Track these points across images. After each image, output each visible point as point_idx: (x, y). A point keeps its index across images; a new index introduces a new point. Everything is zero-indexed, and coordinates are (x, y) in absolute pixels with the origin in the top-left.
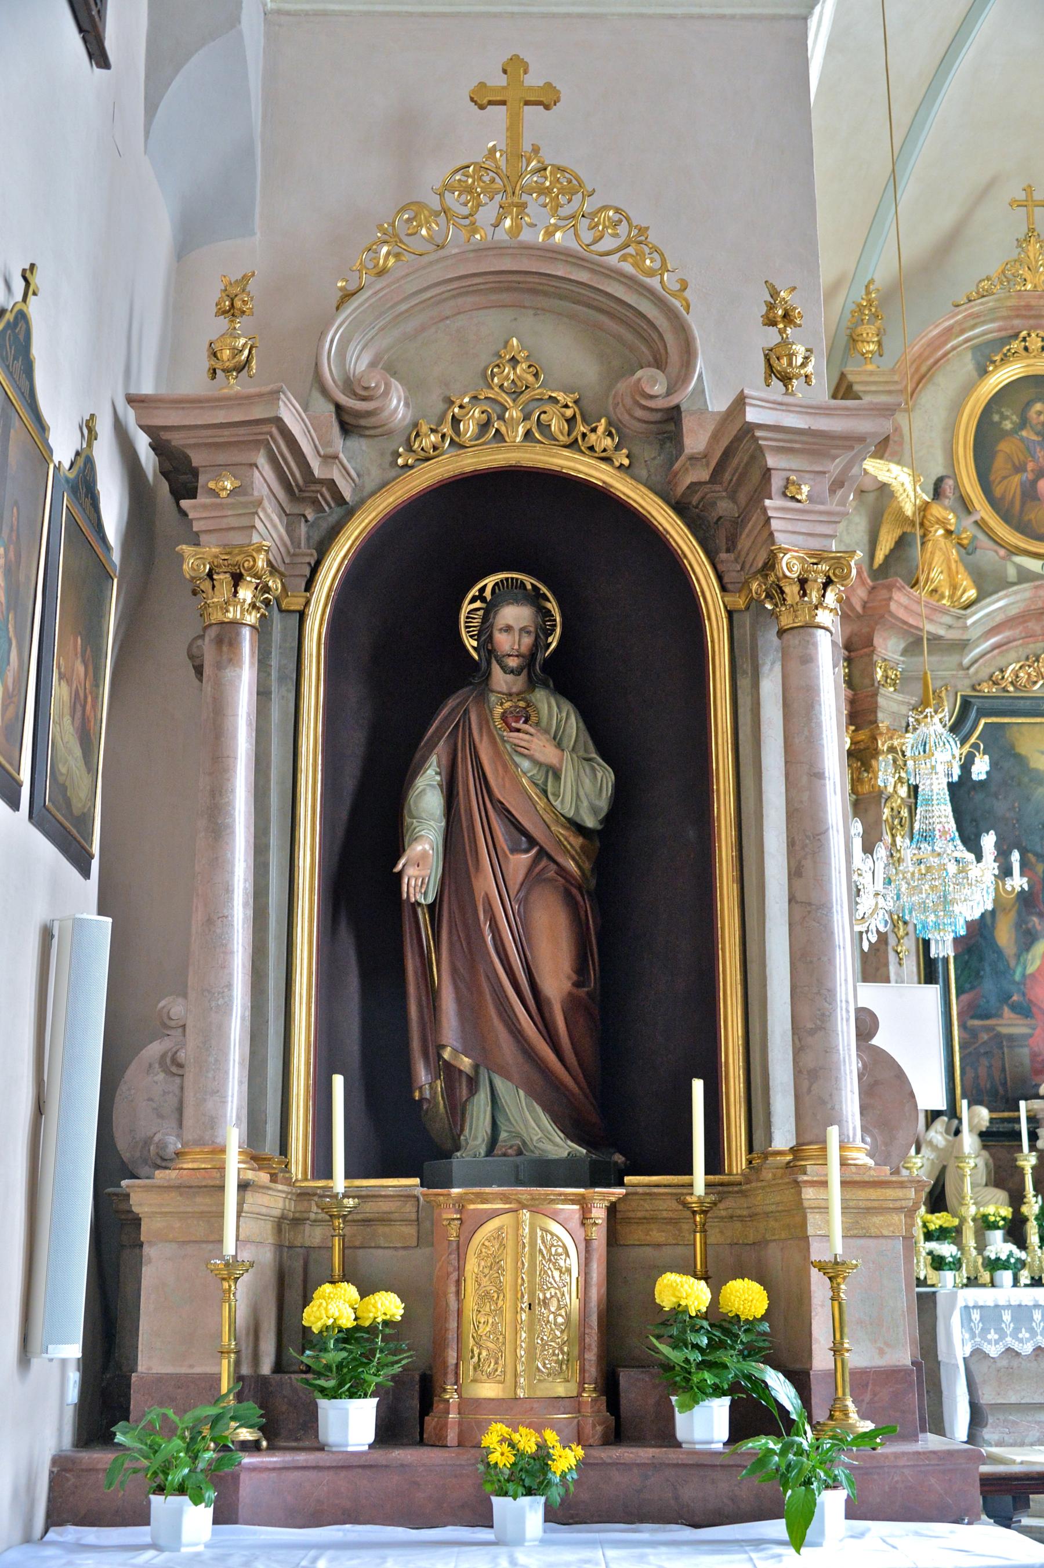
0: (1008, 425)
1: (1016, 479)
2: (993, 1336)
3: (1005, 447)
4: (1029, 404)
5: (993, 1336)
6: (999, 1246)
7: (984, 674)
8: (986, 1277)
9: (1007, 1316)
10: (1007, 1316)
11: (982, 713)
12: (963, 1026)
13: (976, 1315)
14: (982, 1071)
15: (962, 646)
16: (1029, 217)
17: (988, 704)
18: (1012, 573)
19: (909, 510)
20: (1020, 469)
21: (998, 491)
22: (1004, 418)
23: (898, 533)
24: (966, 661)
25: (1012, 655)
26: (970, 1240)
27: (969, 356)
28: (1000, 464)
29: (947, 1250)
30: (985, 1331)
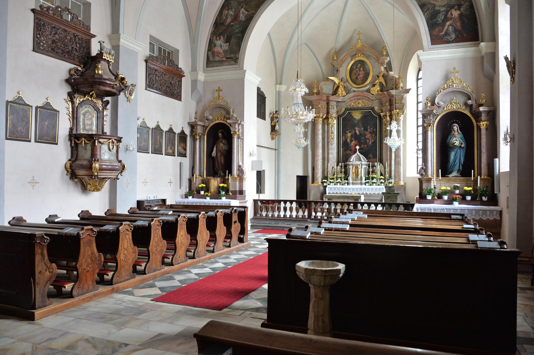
0: (354, 68)
1: (355, 76)
2: (331, 191)
3: (354, 71)
4: (358, 65)
5: (331, 191)
6: (339, 180)
7: (349, 104)
8: (344, 184)
9: (333, 189)
10: (333, 189)
11: (347, 110)
12: (342, 152)
13: (329, 188)
14: (345, 158)
15: (345, 101)
16: (359, 35)
17: (348, 109)
18: (352, 91)
19: (337, 83)
20: (356, 75)
21: (352, 78)
22: (354, 67)
23: (337, 86)
24: (346, 103)
25: (353, 102)
26: (335, 180)
27: (350, 57)
28: (353, 74)
29: (333, 181)
30: (330, 190)
